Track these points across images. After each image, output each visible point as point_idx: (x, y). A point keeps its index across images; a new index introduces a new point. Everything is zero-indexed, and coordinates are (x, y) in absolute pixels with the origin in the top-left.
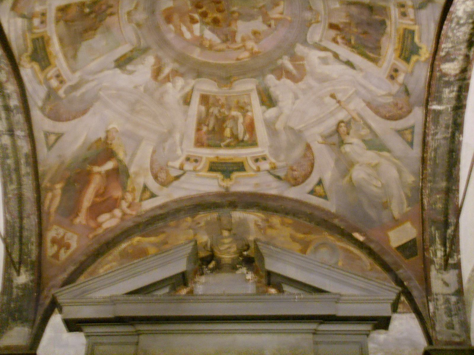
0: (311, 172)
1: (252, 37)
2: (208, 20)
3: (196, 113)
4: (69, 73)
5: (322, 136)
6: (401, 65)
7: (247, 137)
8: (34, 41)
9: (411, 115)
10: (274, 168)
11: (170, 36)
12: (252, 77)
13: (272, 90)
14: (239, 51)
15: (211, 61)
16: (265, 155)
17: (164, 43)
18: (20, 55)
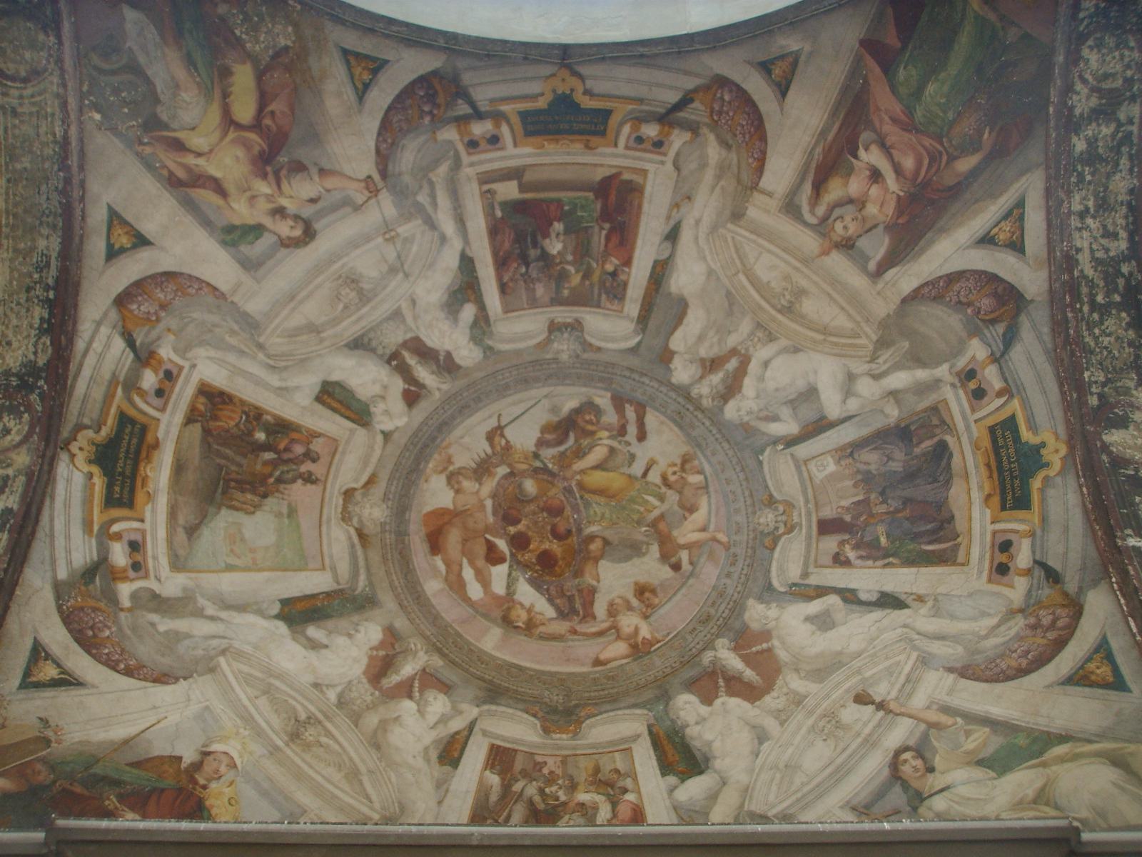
1: (635, 602)
2: (529, 557)
3: (473, 787)
4: (164, 561)
5: (854, 809)
6: (1015, 524)
8: (124, 419)
9: (1083, 620)
11: (432, 587)
12: (635, 706)
13: (692, 731)
14: (601, 640)
15: (528, 665)
18: (79, 427)
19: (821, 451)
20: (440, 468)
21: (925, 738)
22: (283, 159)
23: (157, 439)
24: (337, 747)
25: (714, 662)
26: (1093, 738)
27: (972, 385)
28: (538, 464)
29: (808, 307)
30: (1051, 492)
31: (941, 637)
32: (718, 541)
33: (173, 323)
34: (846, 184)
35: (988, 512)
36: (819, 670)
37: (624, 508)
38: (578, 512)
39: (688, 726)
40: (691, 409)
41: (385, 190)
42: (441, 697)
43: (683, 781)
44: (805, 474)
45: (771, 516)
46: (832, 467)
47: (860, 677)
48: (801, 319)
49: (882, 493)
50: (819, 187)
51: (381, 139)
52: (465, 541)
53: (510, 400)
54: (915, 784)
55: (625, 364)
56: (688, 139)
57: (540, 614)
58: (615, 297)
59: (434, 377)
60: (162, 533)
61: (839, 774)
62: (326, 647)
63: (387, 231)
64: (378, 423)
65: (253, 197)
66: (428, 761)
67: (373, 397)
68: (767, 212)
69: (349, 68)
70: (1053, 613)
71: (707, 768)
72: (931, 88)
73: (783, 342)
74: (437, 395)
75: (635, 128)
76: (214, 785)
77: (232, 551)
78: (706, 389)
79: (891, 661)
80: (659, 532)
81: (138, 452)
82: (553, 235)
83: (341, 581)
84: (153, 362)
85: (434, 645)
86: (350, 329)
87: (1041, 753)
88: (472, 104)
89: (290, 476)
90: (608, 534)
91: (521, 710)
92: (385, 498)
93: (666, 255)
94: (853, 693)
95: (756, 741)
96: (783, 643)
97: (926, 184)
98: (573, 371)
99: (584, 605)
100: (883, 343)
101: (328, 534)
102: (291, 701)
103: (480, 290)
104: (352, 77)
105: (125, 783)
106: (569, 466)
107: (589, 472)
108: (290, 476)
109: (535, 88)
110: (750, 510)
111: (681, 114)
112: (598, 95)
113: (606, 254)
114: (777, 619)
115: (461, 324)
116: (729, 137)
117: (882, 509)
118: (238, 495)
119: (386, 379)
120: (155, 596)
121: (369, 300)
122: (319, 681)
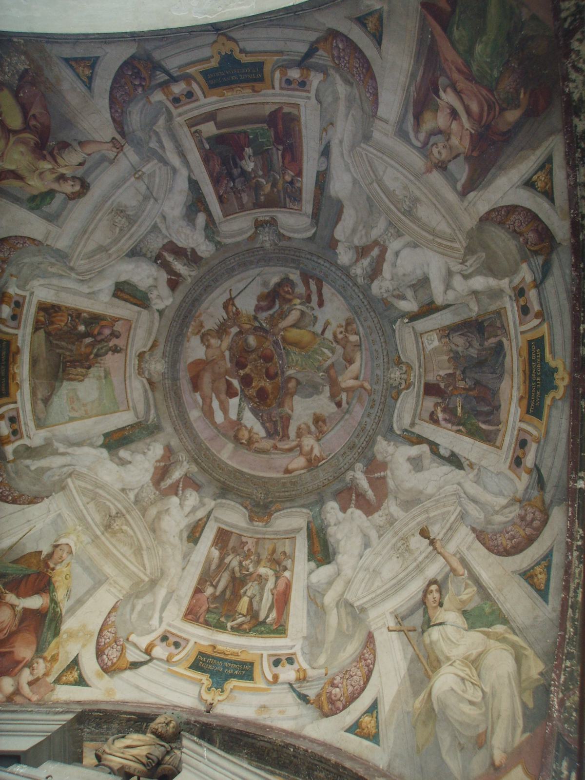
0: (363, 689)
1: (313, 428)
3: (203, 560)
4: (31, 424)
6: (532, 429)
7: (274, 615)
10: (303, 679)
11: (194, 414)
12: (303, 506)
13: (331, 530)
14: (291, 454)
16: (294, 654)
17: (183, 423)
19: (430, 329)
20: (196, 331)
21: (446, 577)
22: (52, 143)
23: (18, 347)
24: (131, 532)
25: (353, 479)
26: (517, 631)
27: (522, 302)
28: (257, 324)
29: (423, 212)
30: (554, 412)
31: (475, 501)
32: (365, 389)
33: (13, 270)
34: (435, 118)
35: (519, 410)
36: (408, 501)
37: (310, 357)
38: (282, 359)
39: (330, 526)
40: (351, 285)
41: (127, 145)
42: (195, 493)
43: (318, 567)
44: (420, 344)
45: (398, 373)
46: (436, 343)
47: (427, 515)
48: (416, 220)
49: (463, 372)
50: (418, 118)
51: (113, 111)
52: (213, 381)
53: (236, 278)
54: (430, 611)
55: (307, 249)
56: (322, 79)
57: (257, 434)
58: (295, 199)
59: (186, 267)
60: (28, 407)
61: (398, 586)
62: (130, 462)
63: (136, 172)
64: (155, 304)
65: (41, 173)
66: (181, 540)
67: (149, 287)
68: (386, 135)
69: (74, 70)
70: (534, 513)
71: (334, 560)
72: (478, 48)
73: (407, 239)
74: (189, 280)
75: (284, 74)
76: (58, 567)
77: (72, 408)
78: (359, 270)
79: (446, 509)
80: (330, 377)
81: (7, 360)
82: (247, 158)
83: (140, 416)
84: (6, 299)
85: (193, 457)
86: (126, 244)
87: (490, 625)
88: (167, 72)
89: (103, 351)
90: (299, 376)
91: (239, 503)
92: (164, 355)
93: (323, 168)
94: (420, 528)
95: (363, 546)
96: (392, 474)
97: (488, 127)
98: (274, 255)
99: (283, 428)
100: (470, 251)
101: (131, 386)
102: (108, 503)
103: (206, 202)
104: (78, 75)
105: (8, 574)
106: (277, 325)
107: (289, 329)
108: (103, 351)
109: (206, 52)
110: (386, 367)
111: (313, 60)
112: (250, 53)
113: (284, 168)
114: (392, 455)
115: (198, 227)
116: (349, 77)
117: (461, 384)
118: (73, 371)
119: (155, 274)
120: (28, 448)
121: (135, 222)
122: (125, 487)
